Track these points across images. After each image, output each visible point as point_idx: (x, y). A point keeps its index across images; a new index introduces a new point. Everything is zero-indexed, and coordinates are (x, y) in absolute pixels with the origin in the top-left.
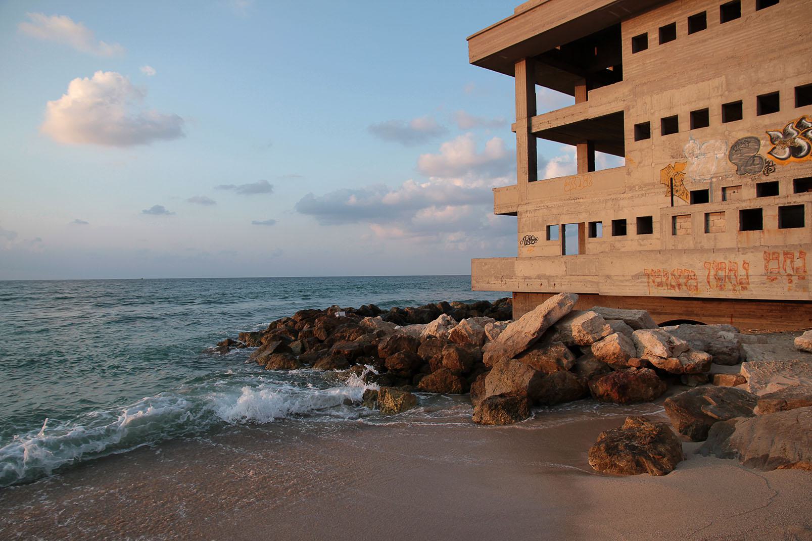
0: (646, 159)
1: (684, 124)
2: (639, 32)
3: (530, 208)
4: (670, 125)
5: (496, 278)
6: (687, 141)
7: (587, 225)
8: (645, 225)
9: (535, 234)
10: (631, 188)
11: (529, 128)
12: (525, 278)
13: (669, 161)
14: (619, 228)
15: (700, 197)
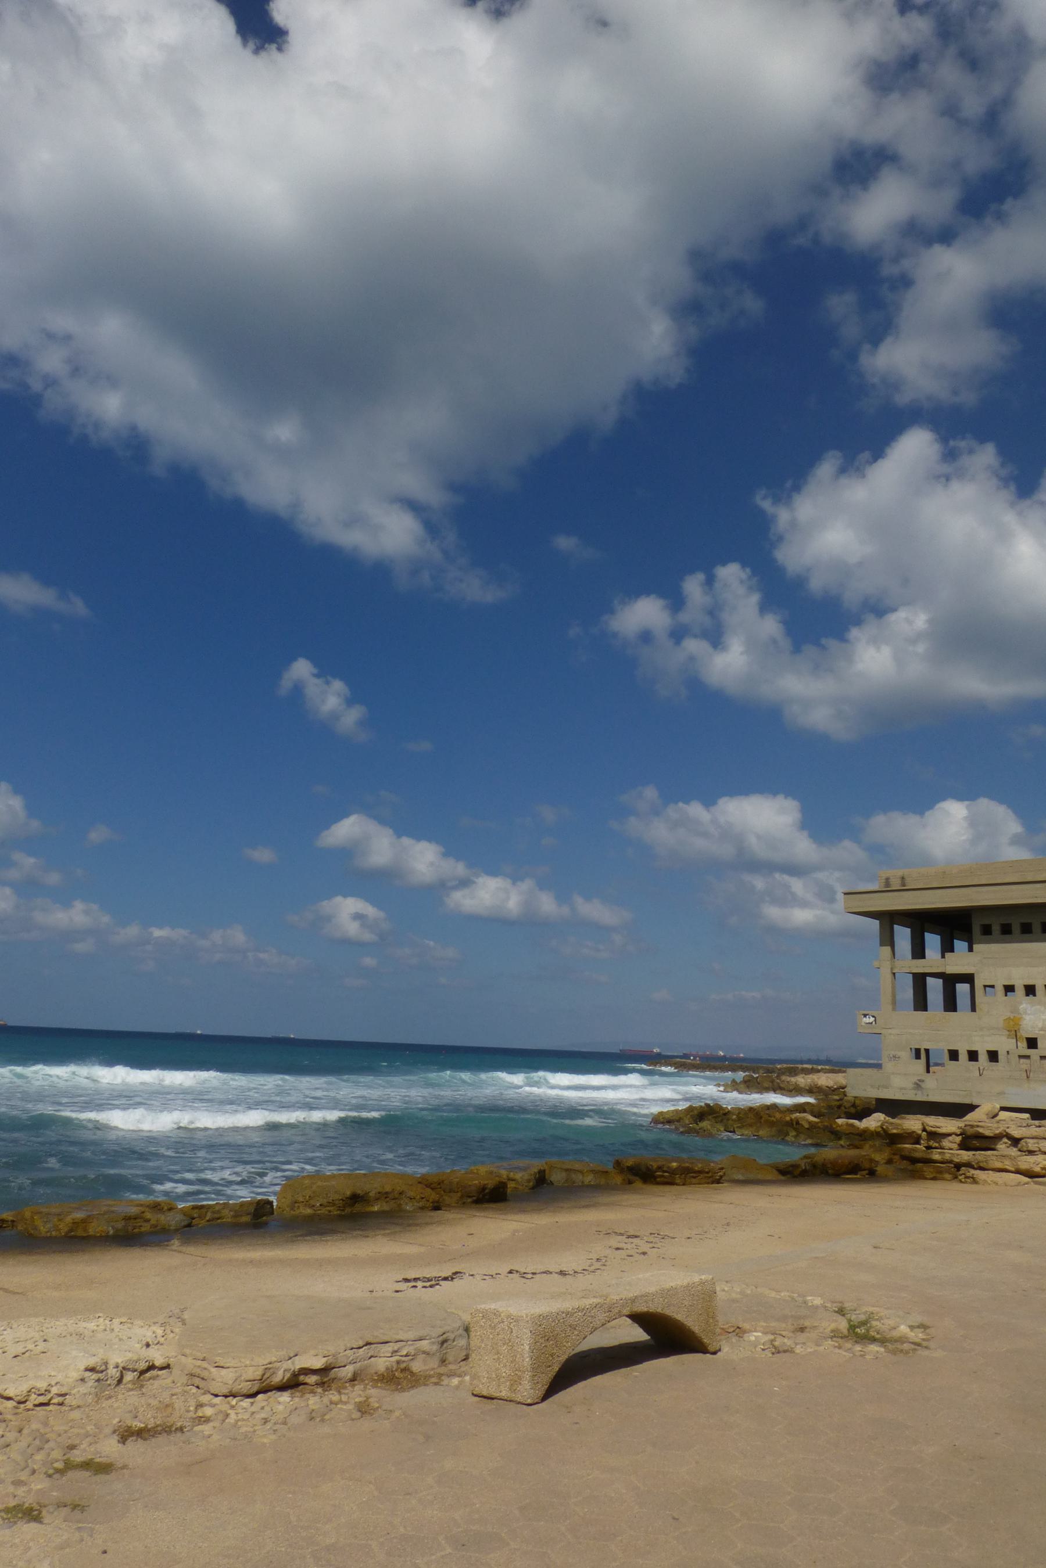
0: (994, 1009)
1: (1020, 991)
2: (987, 922)
3: (893, 1031)
4: (1009, 989)
5: (872, 1086)
6: (1021, 1003)
7: (946, 1052)
8: (993, 1056)
9: (899, 1054)
10: (981, 1029)
11: (892, 969)
12: (901, 1089)
13: (1009, 1014)
14: (973, 1056)
15: (1032, 1043)
